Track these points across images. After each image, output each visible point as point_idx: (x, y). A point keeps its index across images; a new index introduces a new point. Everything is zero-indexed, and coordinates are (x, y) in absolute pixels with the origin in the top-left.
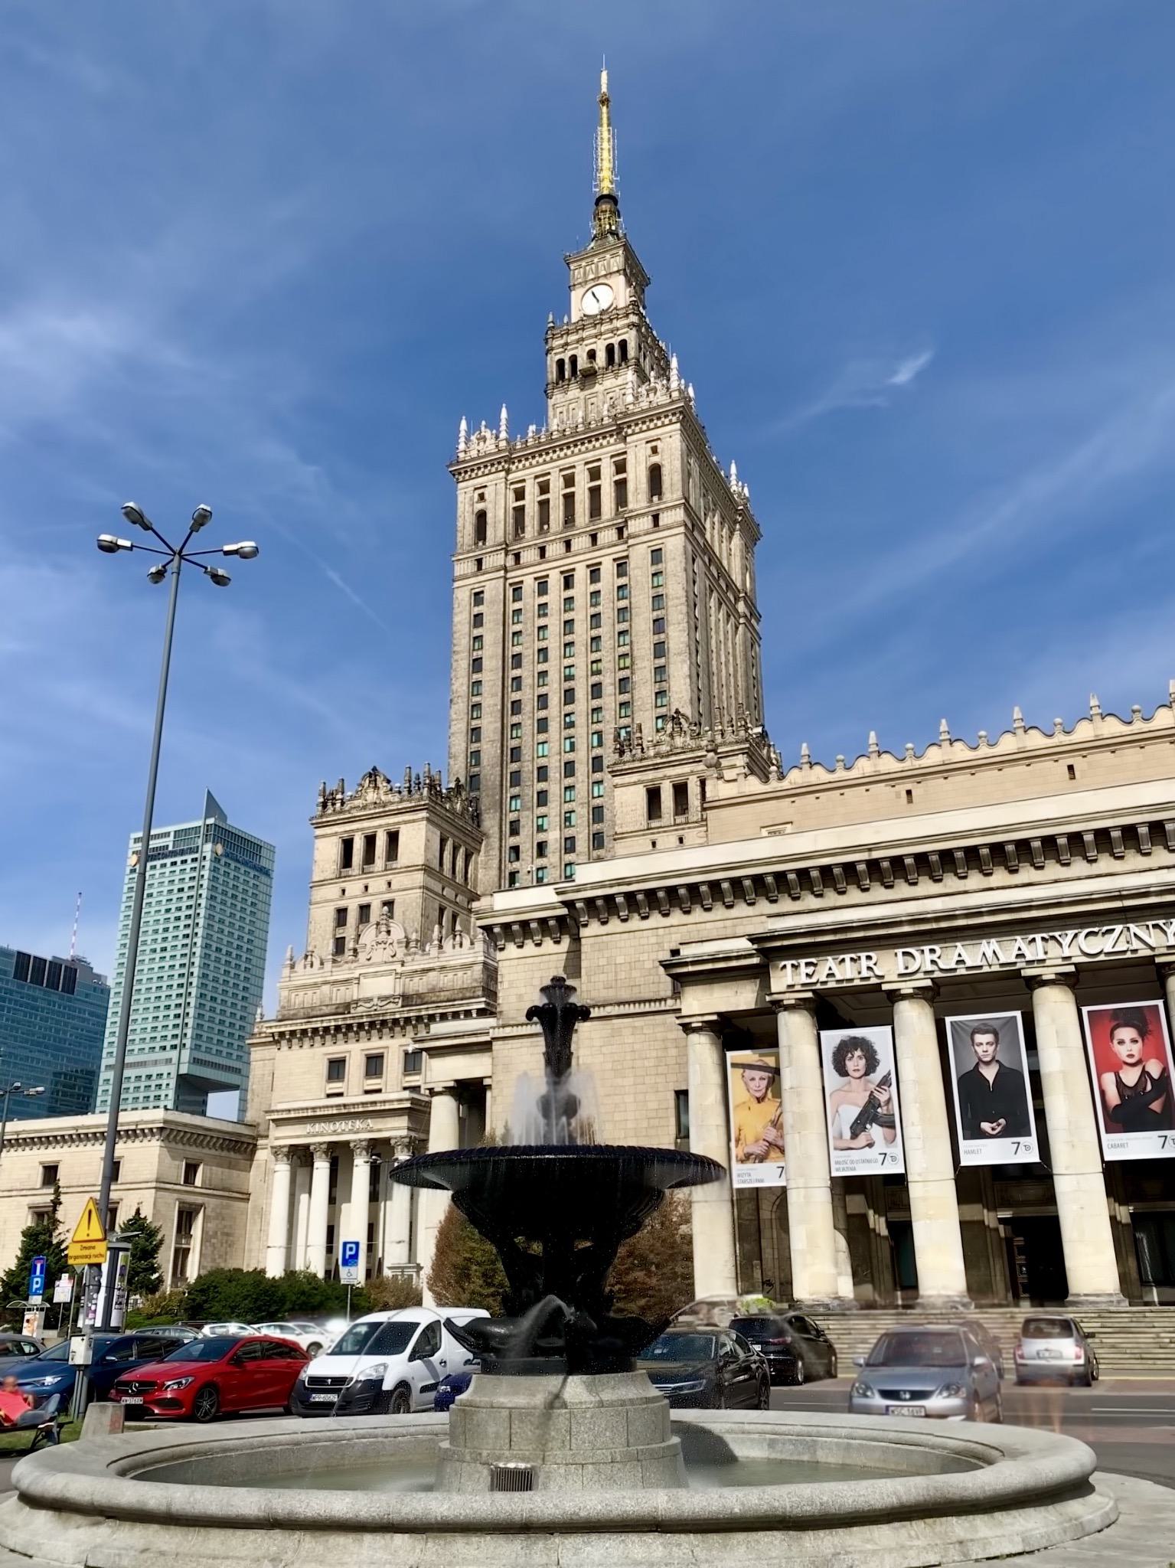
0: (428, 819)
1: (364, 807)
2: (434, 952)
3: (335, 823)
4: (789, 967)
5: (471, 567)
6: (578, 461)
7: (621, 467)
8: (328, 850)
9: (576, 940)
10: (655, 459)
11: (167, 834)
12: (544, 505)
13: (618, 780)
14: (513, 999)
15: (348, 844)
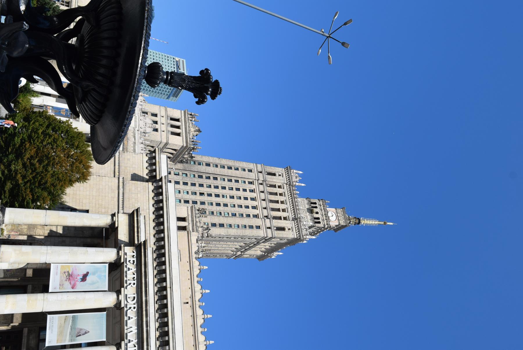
0: (183, 146)
1: (189, 127)
2: (141, 141)
3: (185, 117)
4: (133, 254)
5: (260, 170)
6: (288, 206)
7: (285, 218)
8: (177, 113)
9: (147, 181)
10: (287, 229)
11: (184, 70)
12: (276, 194)
13: (189, 208)
14: (129, 157)
15: (178, 120)
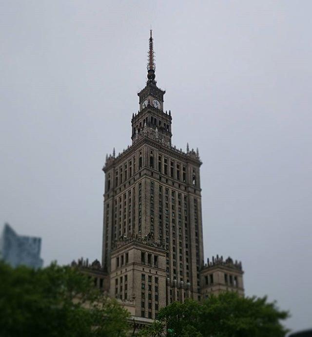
7: (184, 169)
